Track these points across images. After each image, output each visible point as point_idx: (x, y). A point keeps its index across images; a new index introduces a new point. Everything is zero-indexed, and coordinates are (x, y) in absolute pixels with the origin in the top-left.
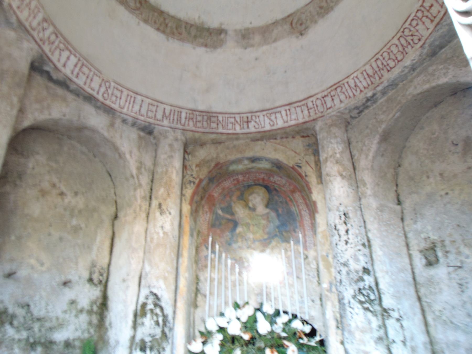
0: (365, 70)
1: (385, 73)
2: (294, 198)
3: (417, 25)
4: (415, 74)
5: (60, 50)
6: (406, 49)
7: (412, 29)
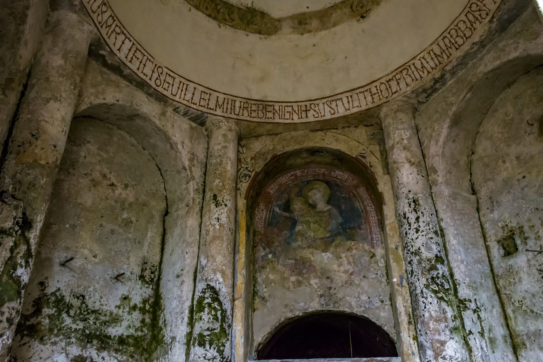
0: (432, 50)
1: (453, 51)
2: (358, 194)
4: (485, 51)
5: (116, 33)
6: (474, 25)
7: (479, 4)
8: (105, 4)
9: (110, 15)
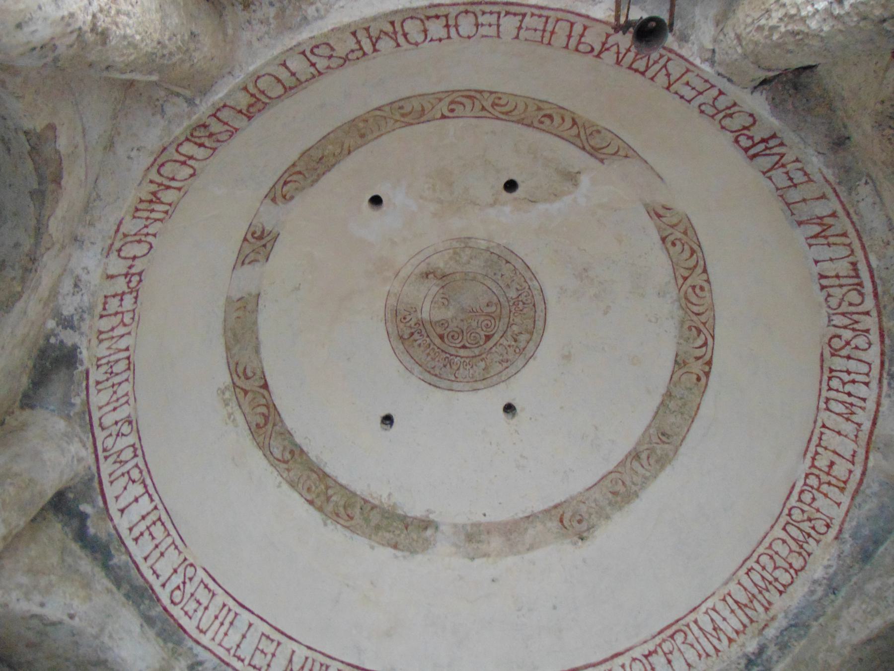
0: (729, 595)
1: (773, 596)
3: (814, 499)
4: (839, 601)
5: (130, 478)
6: (805, 545)
7: (806, 508)
8: (130, 423)
9: (132, 443)
